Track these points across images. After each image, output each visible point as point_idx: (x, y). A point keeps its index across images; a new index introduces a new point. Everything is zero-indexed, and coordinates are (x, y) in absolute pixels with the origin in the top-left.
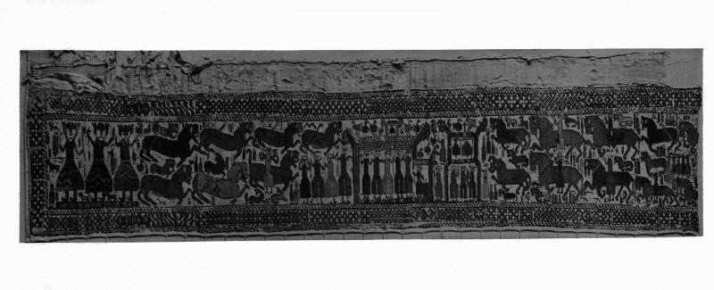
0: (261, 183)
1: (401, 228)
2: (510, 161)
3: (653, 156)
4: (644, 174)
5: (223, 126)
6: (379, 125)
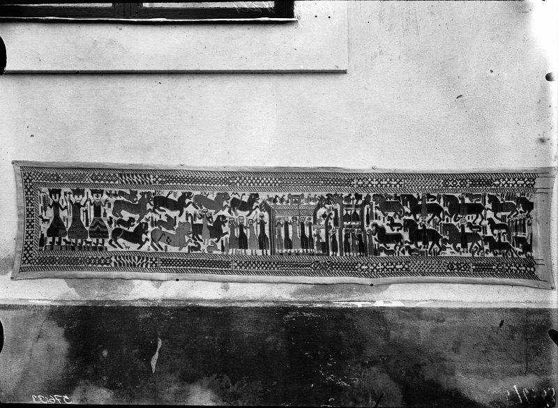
0: (200, 237)
5: (169, 194)
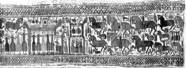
1: (49, 65)
2: (98, 36)
3: (163, 33)
4: (159, 41)
6: (39, 20)
